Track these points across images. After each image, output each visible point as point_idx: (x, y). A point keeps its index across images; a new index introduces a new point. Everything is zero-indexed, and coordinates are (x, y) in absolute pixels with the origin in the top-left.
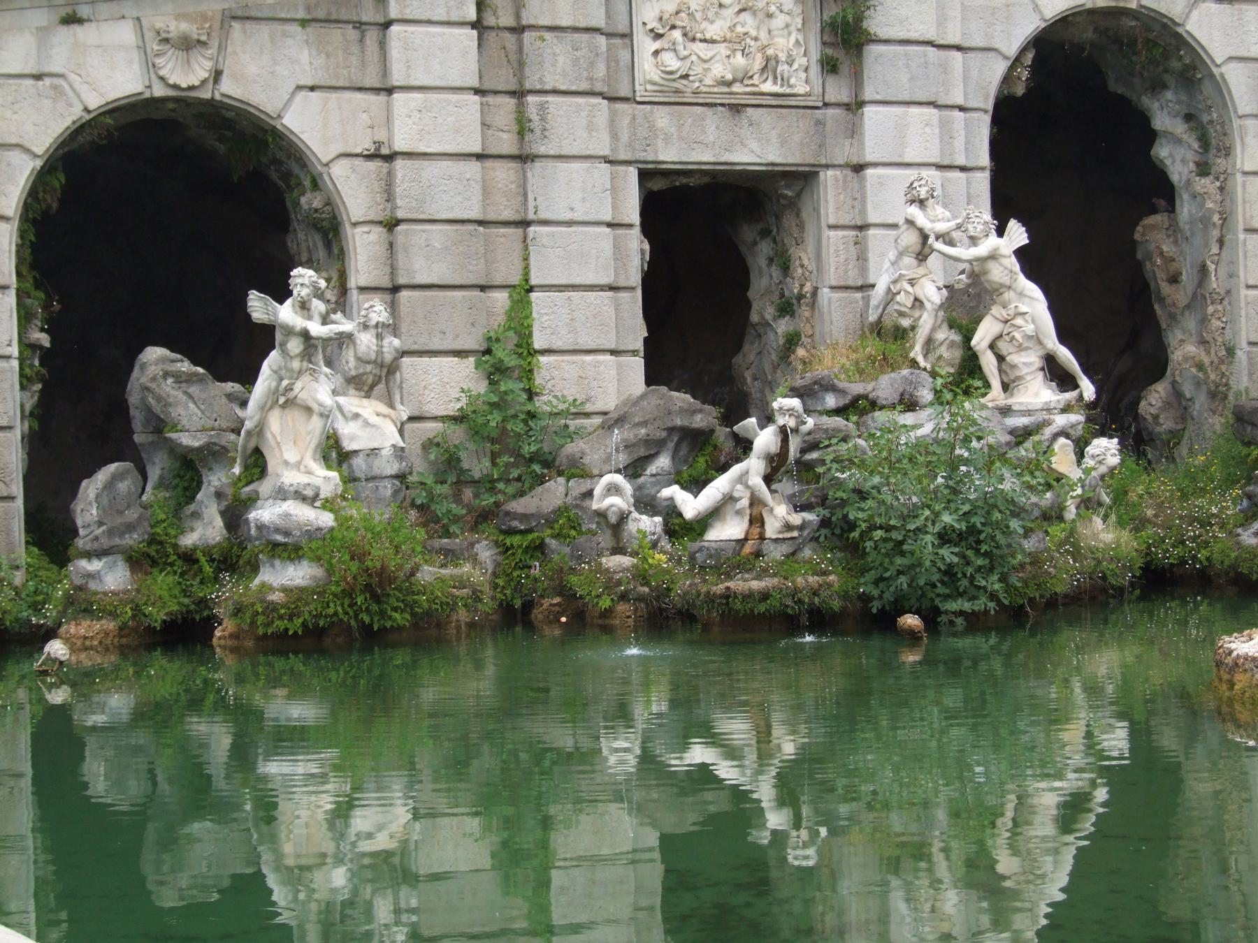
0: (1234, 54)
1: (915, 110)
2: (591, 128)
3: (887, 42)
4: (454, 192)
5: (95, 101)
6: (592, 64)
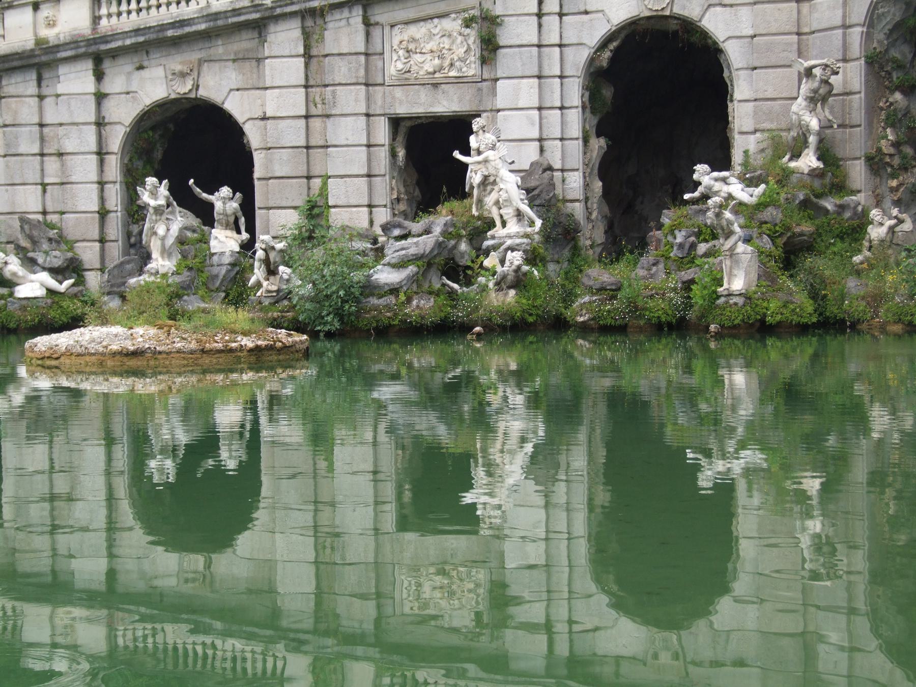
0: (731, 35)
1: (525, 81)
2: (356, 100)
3: (510, 47)
4: (294, 133)
5: (155, 100)
6: (357, 70)
